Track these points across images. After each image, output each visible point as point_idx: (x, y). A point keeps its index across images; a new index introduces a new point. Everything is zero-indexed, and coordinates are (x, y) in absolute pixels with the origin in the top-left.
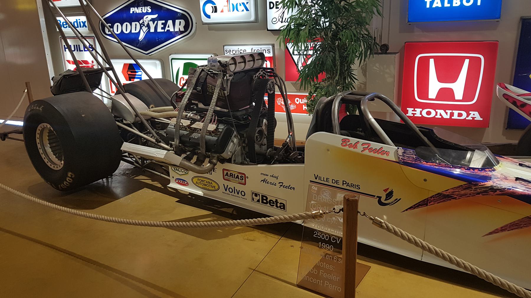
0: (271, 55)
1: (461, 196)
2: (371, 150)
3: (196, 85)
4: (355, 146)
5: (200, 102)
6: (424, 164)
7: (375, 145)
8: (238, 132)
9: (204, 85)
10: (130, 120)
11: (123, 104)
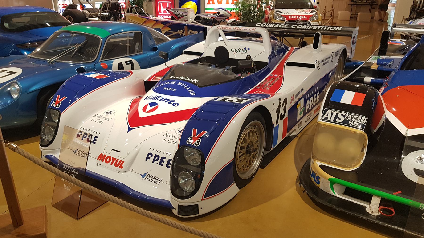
0: (125, 2)
1: (147, 21)
2: (135, 15)
3: (104, 5)
4: (132, 15)
5: (105, 10)
6: (142, 17)
7: (135, 14)
8: (113, 15)
9: (106, 5)
10: (88, 16)
11: (86, 12)
